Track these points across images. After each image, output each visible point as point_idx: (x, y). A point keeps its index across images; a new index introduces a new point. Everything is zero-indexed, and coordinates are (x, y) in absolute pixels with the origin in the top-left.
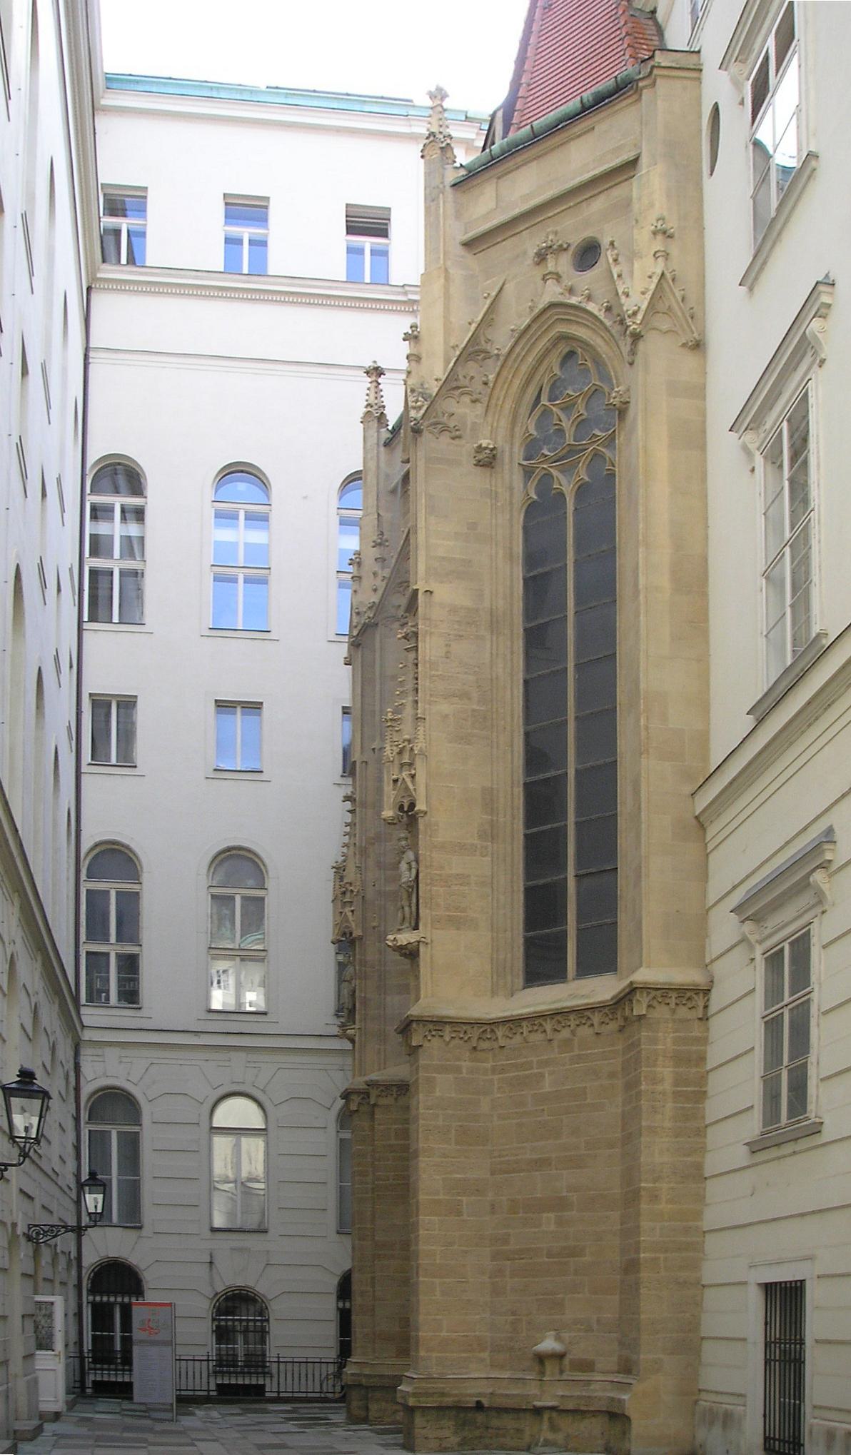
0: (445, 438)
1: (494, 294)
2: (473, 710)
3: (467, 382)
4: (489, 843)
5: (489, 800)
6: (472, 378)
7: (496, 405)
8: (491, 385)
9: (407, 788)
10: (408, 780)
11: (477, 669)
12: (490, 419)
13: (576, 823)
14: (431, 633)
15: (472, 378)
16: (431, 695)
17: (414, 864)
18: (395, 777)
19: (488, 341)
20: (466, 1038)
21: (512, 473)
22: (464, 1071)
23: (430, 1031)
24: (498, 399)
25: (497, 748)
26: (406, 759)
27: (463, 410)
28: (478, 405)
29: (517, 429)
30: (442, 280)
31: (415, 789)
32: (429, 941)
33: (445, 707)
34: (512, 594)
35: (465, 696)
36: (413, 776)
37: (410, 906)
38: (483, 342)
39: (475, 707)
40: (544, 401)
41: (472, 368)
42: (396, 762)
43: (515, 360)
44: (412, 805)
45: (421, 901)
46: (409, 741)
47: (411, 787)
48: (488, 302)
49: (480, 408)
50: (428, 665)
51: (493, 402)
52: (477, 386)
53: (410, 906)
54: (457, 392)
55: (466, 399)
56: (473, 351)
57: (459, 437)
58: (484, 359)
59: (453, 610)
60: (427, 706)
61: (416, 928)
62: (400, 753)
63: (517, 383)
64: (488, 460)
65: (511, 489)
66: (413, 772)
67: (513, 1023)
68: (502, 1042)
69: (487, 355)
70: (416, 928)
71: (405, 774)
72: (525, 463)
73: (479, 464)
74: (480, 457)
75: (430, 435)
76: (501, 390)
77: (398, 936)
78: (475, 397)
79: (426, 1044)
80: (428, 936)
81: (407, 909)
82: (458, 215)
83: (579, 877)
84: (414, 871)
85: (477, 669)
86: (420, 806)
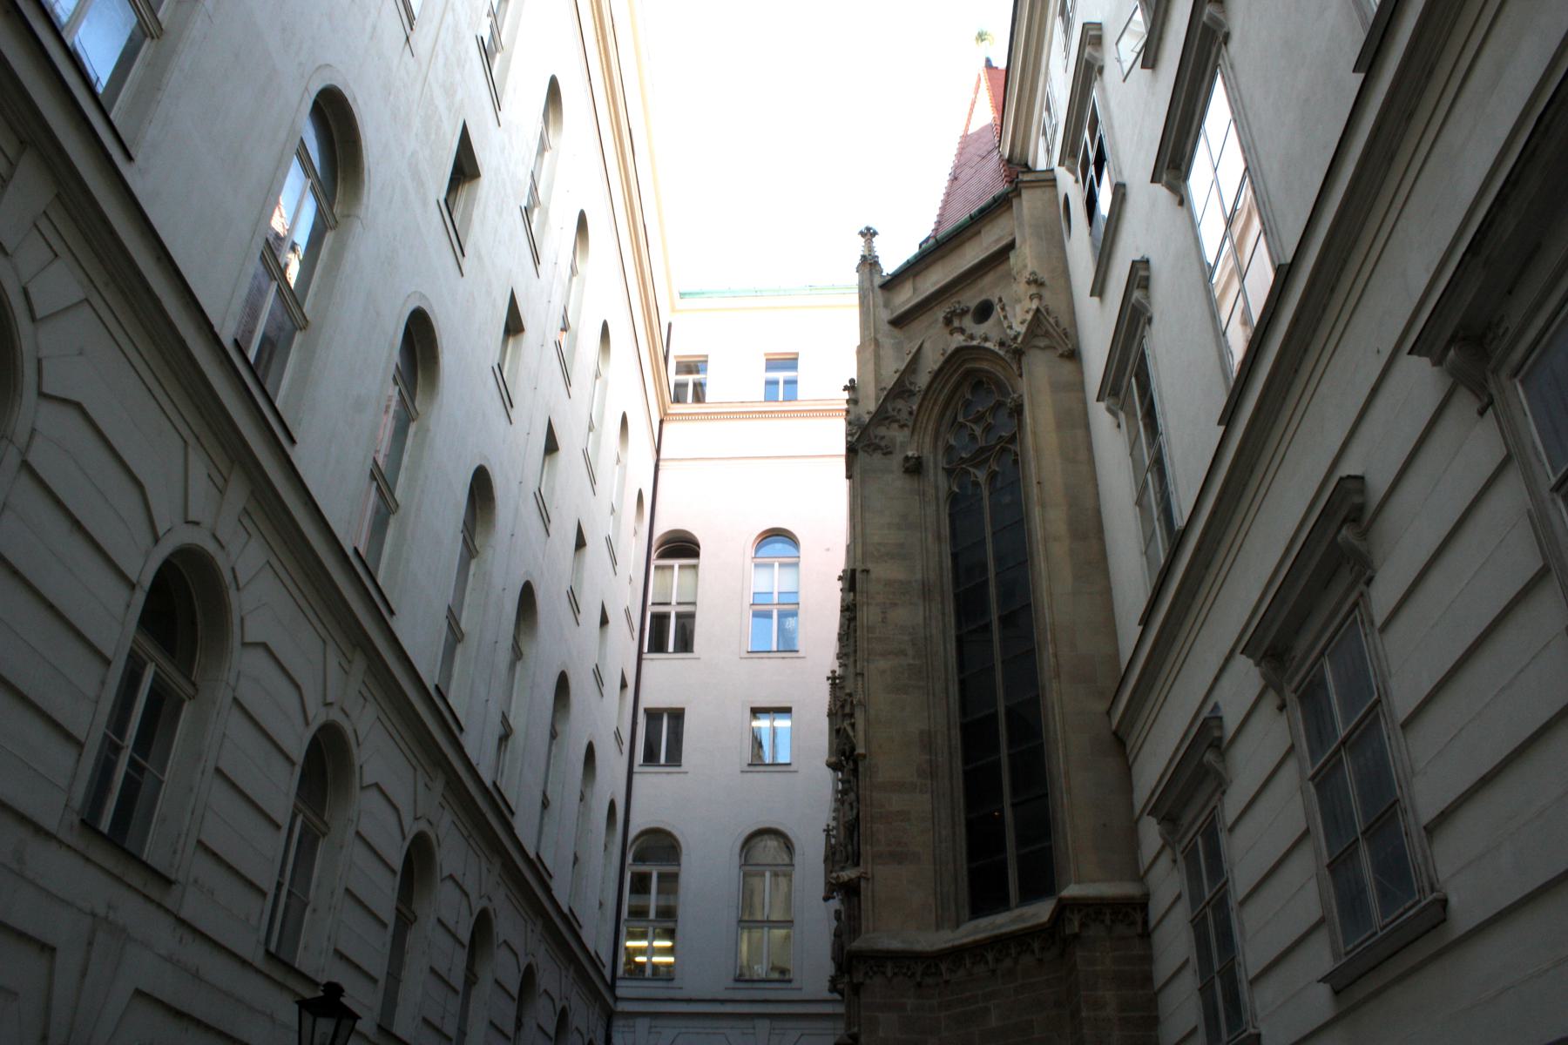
0: (877, 456)
1: (914, 351)
2: (909, 665)
3: (895, 413)
4: (929, 782)
5: (927, 742)
6: (900, 410)
7: (920, 428)
8: (915, 413)
9: (848, 736)
10: (849, 729)
11: (911, 630)
12: (916, 437)
13: (1009, 755)
14: (868, 604)
15: (900, 410)
16: (869, 654)
17: (855, 804)
18: (838, 727)
19: (911, 383)
20: (909, 973)
21: (936, 475)
22: (909, 1008)
23: (871, 968)
24: (922, 423)
25: (934, 695)
26: (847, 710)
27: (897, 435)
28: (906, 429)
29: (940, 443)
30: (873, 347)
31: (854, 736)
32: (870, 876)
33: (882, 664)
34: (941, 568)
35: (903, 653)
36: (853, 725)
37: (852, 845)
38: (908, 385)
39: (911, 662)
40: (961, 419)
41: (900, 404)
42: (840, 713)
43: (933, 394)
44: (853, 749)
45: (861, 838)
46: (850, 695)
47: (851, 734)
48: (910, 356)
49: (907, 432)
50: (865, 630)
51: (918, 425)
52: (904, 415)
53: (852, 845)
54: (887, 422)
55: (895, 426)
56: (900, 390)
57: (891, 453)
58: (909, 396)
59: (889, 583)
60: (866, 664)
61: (857, 864)
62: (843, 707)
63: (937, 409)
64: (914, 468)
65: (937, 488)
66: (853, 721)
67: (956, 955)
68: (946, 976)
69: (912, 394)
70: (857, 864)
71: (846, 724)
72: (947, 467)
73: (907, 471)
74: (907, 465)
75: (866, 455)
76: (924, 415)
77: (841, 874)
78: (902, 423)
79: (868, 981)
80: (869, 870)
81: (849, 847)
82: (886, 305)
83: (1014, 805)
84: (855, 811)
85: (911, 630)
86: (860, 750)
